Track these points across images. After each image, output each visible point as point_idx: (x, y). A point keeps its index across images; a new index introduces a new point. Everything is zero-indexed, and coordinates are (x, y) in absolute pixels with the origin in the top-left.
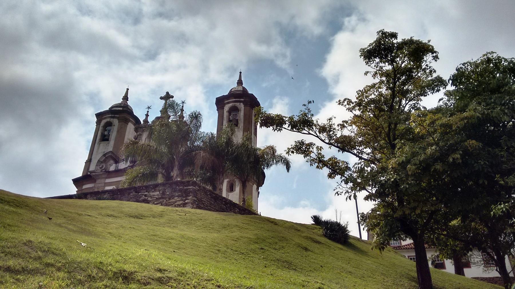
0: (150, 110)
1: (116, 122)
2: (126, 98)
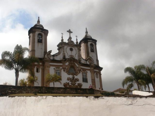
0: (63, 35)
1: (43, 34)
2: (39, 22)
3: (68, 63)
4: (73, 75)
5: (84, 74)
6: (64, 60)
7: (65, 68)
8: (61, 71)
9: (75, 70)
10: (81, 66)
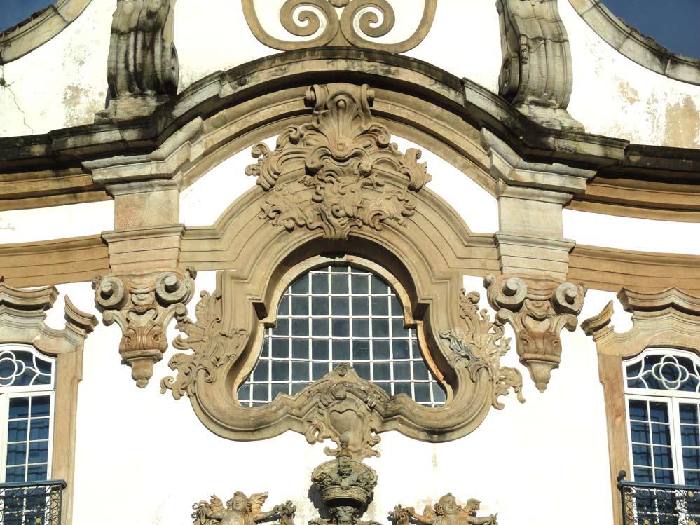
3: (252, 181)
4: (338, 429)
5: (674, 398)
6: (123, 125)
7: (168, 298)
8: (77, 379)
9: (421, 311)
10: (576, 199)
